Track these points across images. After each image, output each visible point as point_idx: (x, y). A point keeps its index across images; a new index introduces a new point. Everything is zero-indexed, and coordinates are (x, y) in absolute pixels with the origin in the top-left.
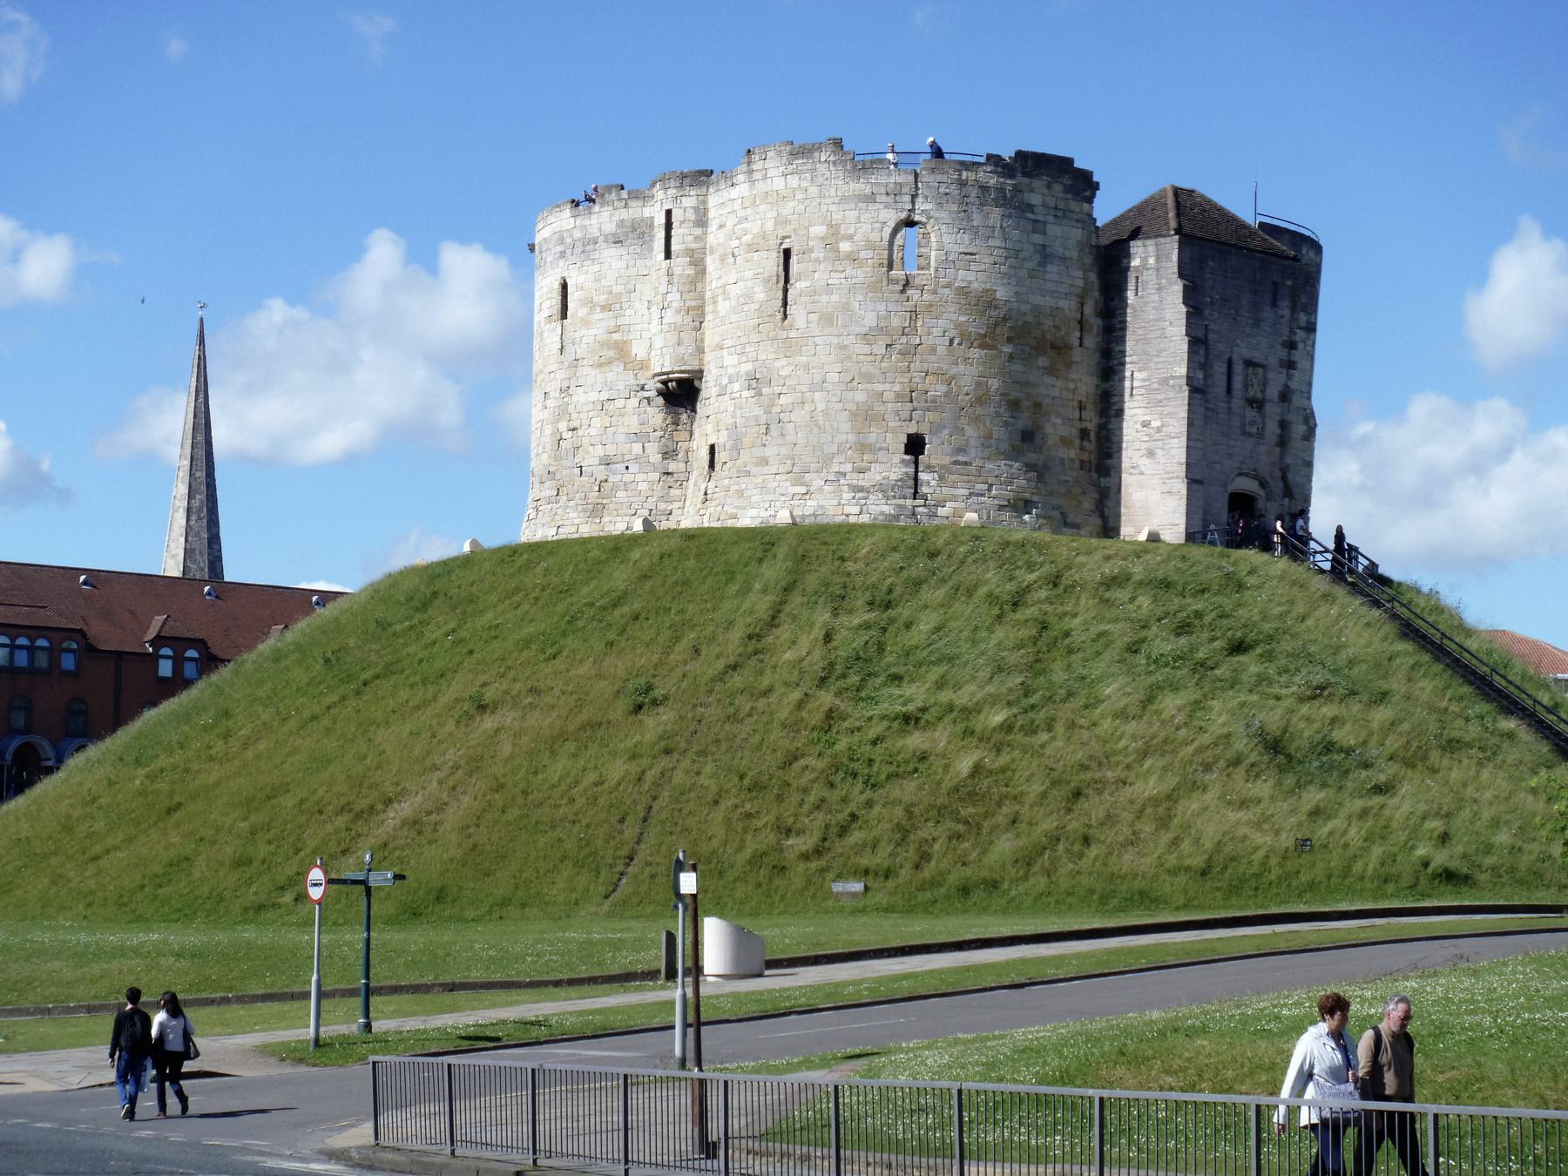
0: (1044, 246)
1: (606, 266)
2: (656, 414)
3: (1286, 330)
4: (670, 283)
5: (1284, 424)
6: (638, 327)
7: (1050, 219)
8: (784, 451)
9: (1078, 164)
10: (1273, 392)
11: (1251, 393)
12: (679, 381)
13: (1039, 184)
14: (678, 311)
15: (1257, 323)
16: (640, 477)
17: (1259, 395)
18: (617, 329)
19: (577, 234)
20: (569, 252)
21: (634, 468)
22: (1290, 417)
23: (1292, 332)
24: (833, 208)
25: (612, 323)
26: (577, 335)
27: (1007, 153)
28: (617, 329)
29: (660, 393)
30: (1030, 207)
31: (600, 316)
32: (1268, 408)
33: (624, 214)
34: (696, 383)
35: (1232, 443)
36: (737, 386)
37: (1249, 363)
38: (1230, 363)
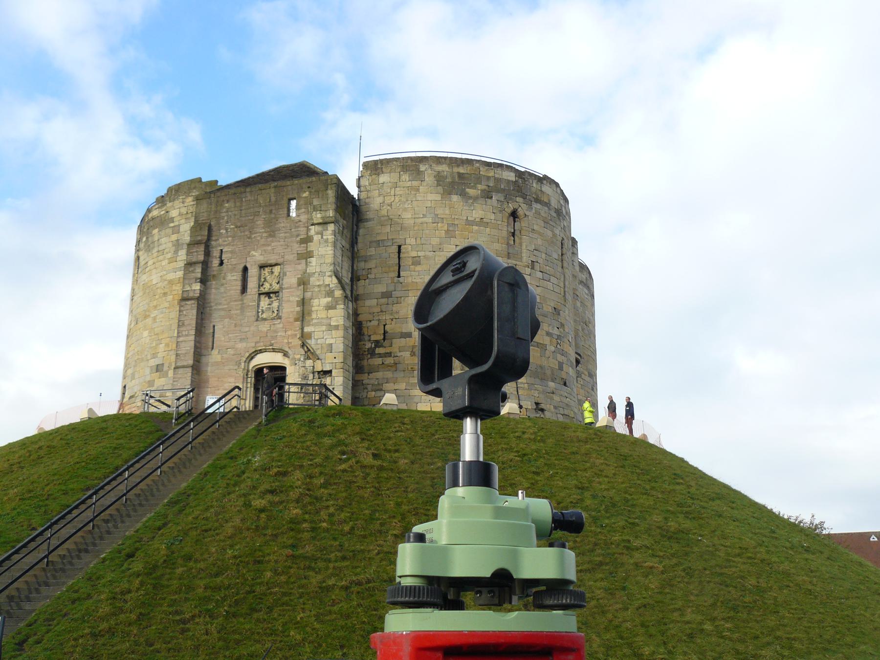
0: (178, 240)
3: (303, 230)
5: (303, 303)
7: (183, 221)
9: (204, 180)
10: (291, 280)
11: (267, 287)
13: (177, 203)
15: (272, 234)
17: (276, 287)
22: (308, 295)
23: (308, 230)
27: (163, 192)
30: (172, 220)
32: (285, 294)
35: (247, 329)
37: (262, 267)
38: (245, 269)
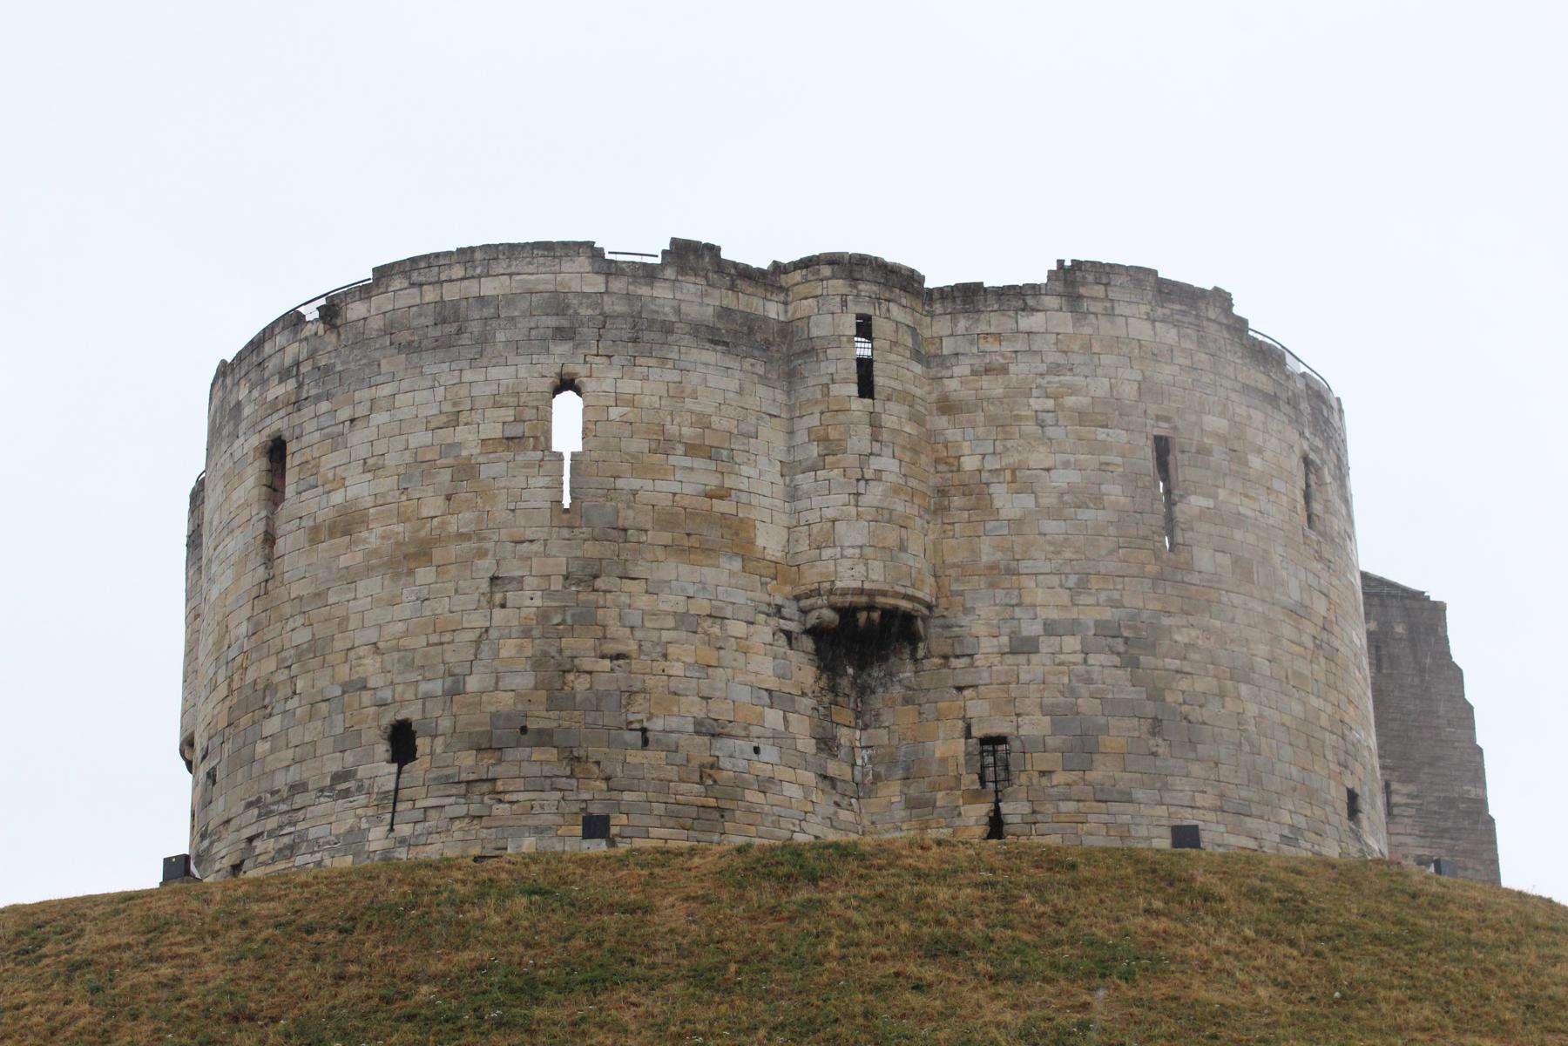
1: (694, 379)
2: (805, 673)
4: (875, 438)
6: (767, 502)
8: (1196, 769)
12: (890, 614)
14: (896, 490)
16: (783, 773)
18: (722, 494)
19: (610, 305)
20: (588, 332)
21: (769, 753)
24: (1233, 396)
25: (713, 481)
26: (620, 483)
28: (722, 494)
29: (815, 632)
31: (687, 462)
33: (730, 300)
34: (920, 623)
36: (1072, 643)
